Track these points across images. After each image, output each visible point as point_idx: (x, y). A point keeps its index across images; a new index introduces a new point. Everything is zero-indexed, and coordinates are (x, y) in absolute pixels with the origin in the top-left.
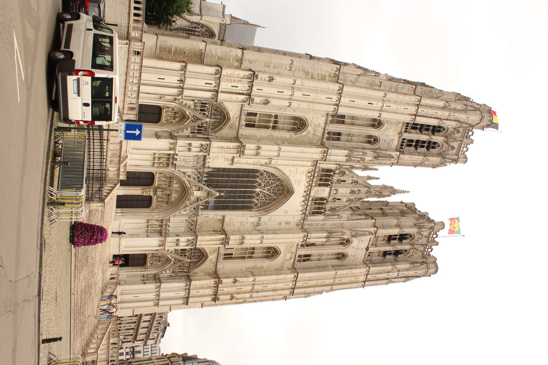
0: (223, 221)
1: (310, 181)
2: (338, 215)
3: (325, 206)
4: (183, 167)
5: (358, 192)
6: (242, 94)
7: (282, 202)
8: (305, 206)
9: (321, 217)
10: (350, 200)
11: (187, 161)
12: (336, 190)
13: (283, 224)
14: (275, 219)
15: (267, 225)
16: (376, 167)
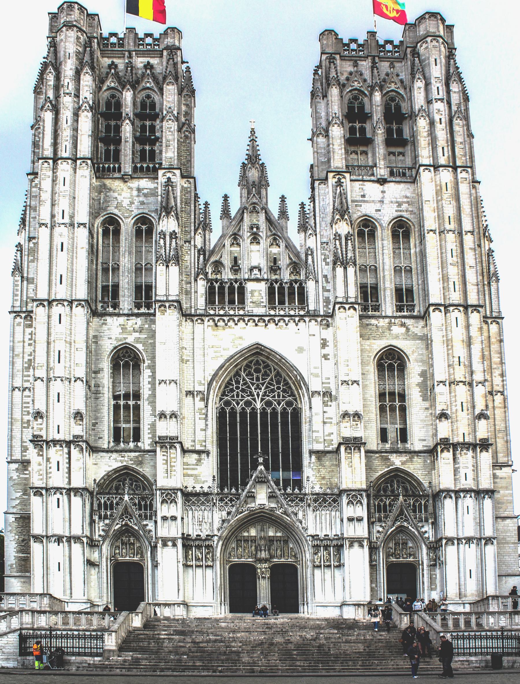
0: (320, 454)
1: (234, 321)
2: (307, 255)
3: (286, 283)
4: (212, 524)
5: (255, 230)
6: (69, 453)
7: (280, 361)
8: (287, 319)
9: (310, 286)
10: (275, 239)
11: (201, 520)
12: (251, 270)
13: (325, 351)
14: (315, 368)
15: (329, 379)
16: (202, 207)
